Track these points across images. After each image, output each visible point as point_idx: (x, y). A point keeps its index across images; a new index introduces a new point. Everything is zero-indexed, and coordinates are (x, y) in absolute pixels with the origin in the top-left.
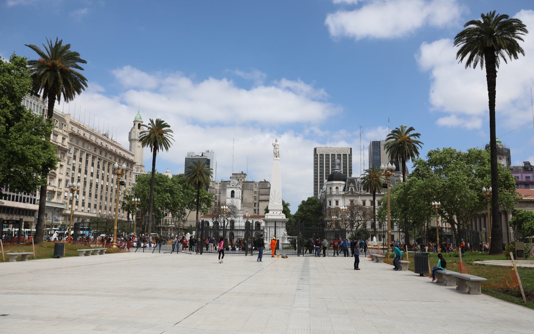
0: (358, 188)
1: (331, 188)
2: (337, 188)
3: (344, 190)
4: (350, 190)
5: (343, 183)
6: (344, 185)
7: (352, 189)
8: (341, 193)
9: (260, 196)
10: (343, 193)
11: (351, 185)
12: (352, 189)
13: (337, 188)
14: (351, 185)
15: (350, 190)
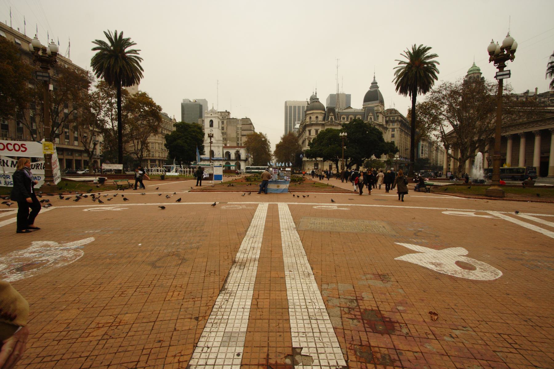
0: (338, 117)
1: (310, 118)
2: (317, 117)
3: (324, 119)
4: (330, 120)
5: (323, 112)
6: (323, 115)
7: (332, 119)
8: (321, 122)
9: (242, 132)
10: (323, 122)
11: (332, 114)
12: (332, 119)
13: (317, 117)
14: (332, 114)
15: (330, 120)
